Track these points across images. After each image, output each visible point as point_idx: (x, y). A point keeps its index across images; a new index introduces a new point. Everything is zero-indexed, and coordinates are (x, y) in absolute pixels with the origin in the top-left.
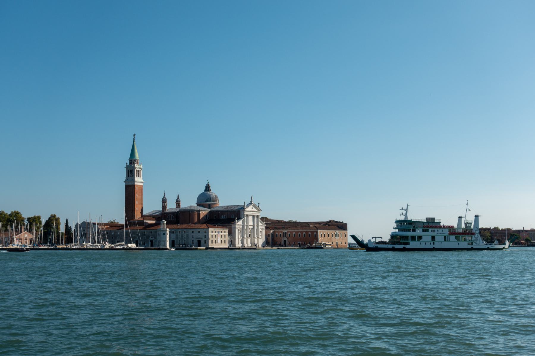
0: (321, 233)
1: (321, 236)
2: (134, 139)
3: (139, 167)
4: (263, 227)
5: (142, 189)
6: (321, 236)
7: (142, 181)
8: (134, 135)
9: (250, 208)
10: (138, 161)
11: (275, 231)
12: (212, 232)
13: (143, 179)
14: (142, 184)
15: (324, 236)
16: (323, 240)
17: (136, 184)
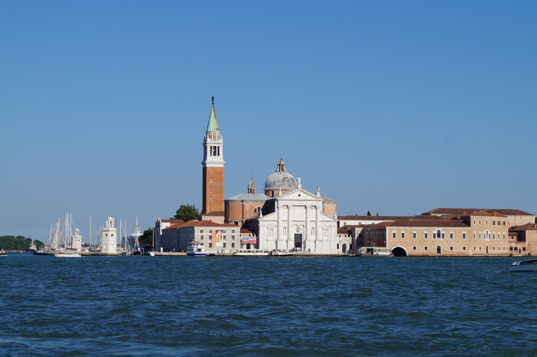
0: (394, 232)
1: (394, 236)
2: (213, 103)
3: (217, 142)
4: (330, 223)
5: (222, 172)
6: (394, 236)
7: (223, 161)
8: (213, 98)
9: (294, 195)
10: (214, 134)
11: (364, 229)
12: (201, 231)
13: (224, 159)
14: (222, 166)
15: (494, 238)
16: (399, 242)
17: (208, 166)
